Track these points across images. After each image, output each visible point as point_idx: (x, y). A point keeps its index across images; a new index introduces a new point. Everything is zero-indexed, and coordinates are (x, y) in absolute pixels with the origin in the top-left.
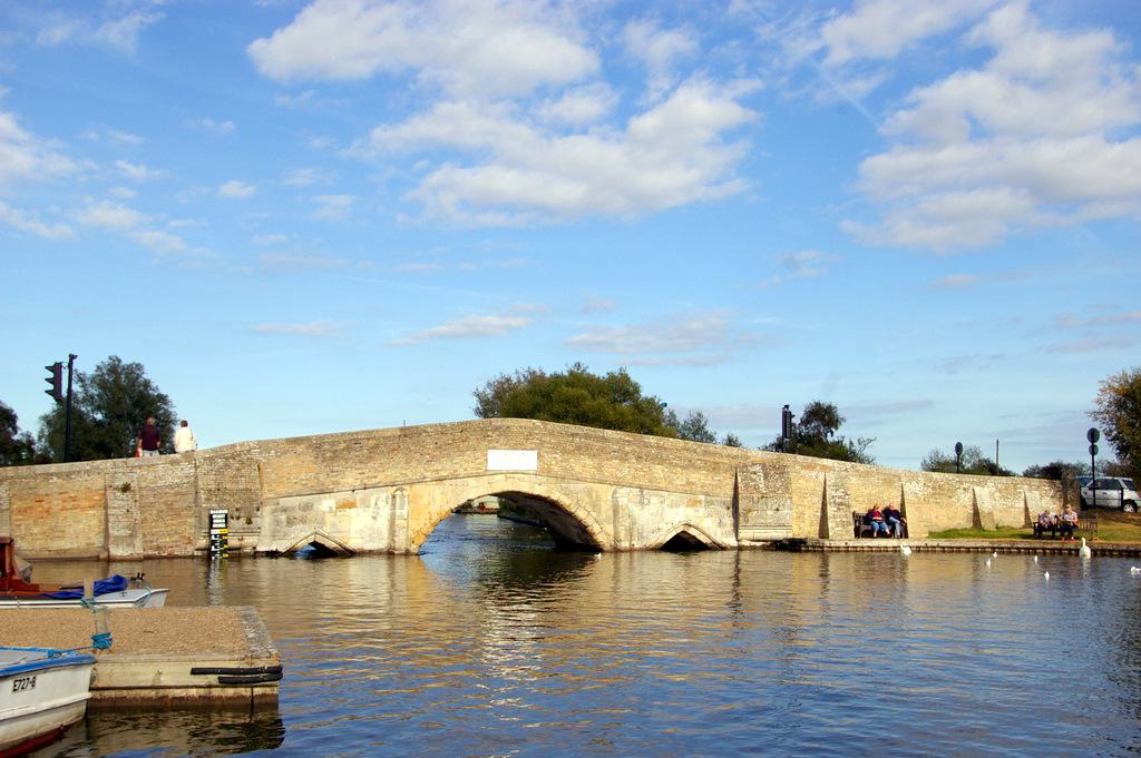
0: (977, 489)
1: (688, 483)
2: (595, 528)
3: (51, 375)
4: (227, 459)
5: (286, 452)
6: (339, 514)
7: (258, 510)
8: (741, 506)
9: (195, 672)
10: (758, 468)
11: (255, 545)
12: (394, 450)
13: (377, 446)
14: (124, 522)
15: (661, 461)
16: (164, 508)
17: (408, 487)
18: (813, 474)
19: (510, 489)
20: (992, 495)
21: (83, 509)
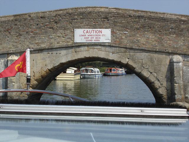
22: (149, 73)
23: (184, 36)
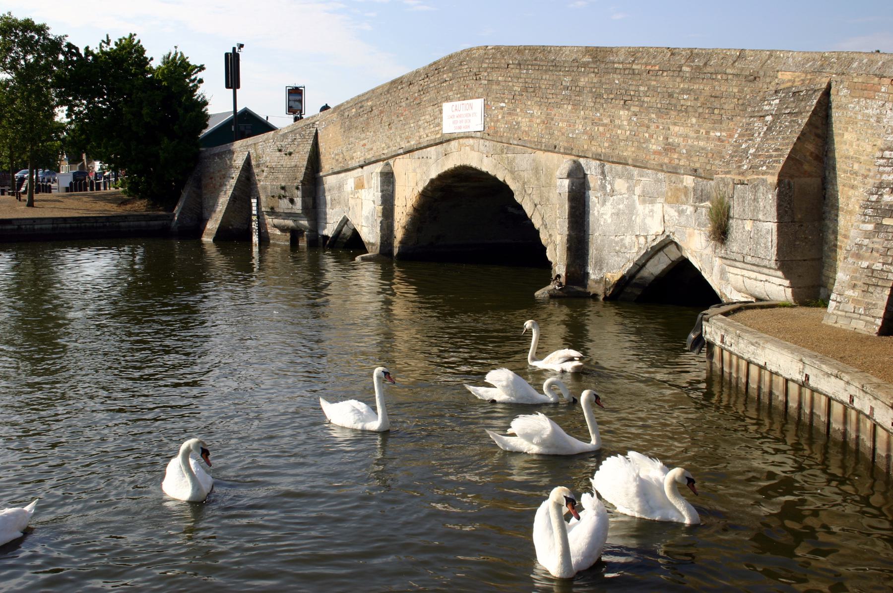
1: (669, 148)
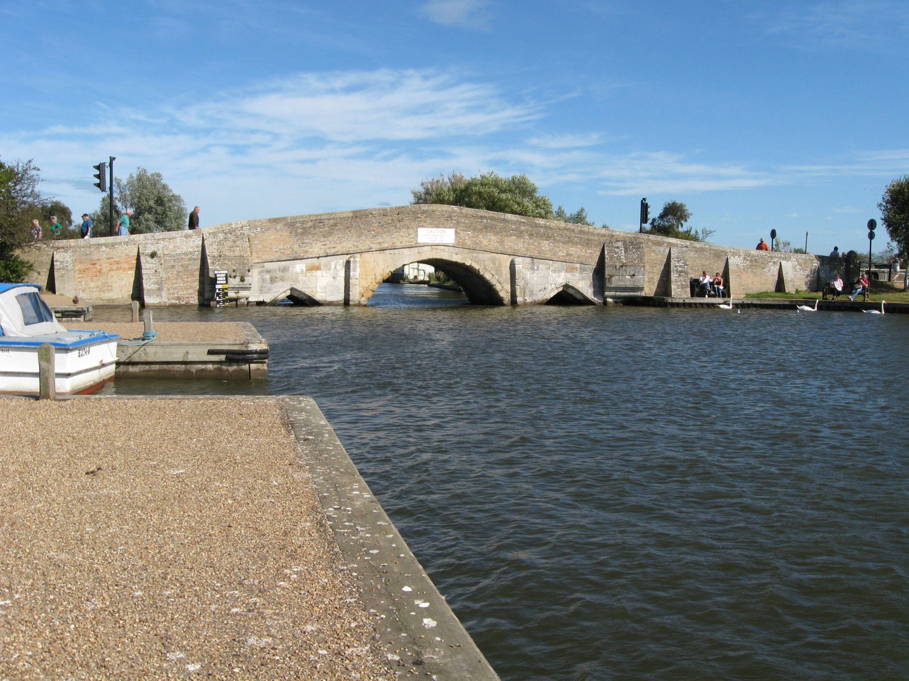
0: (783, 263)
1: (568, 255)
2: (498, 287)
3: (97, 172)
4: (225, 233)
5: (269, 229)
6: (309, 275)
7: (249, 271)
8: (608, 272)
9: (211, 352)
10: (620, 244)
11: (247, 297)
12: (348, 228)
13: (336, 225)
14: (154, 279)
15: (548, 238)
16: (181, 269)
17: (358, 255)
18: (662, 249)
19: (435, 257)
20: (794, 267)
21: (124, 270)
22: (491, 276)
23: (523, 239)
